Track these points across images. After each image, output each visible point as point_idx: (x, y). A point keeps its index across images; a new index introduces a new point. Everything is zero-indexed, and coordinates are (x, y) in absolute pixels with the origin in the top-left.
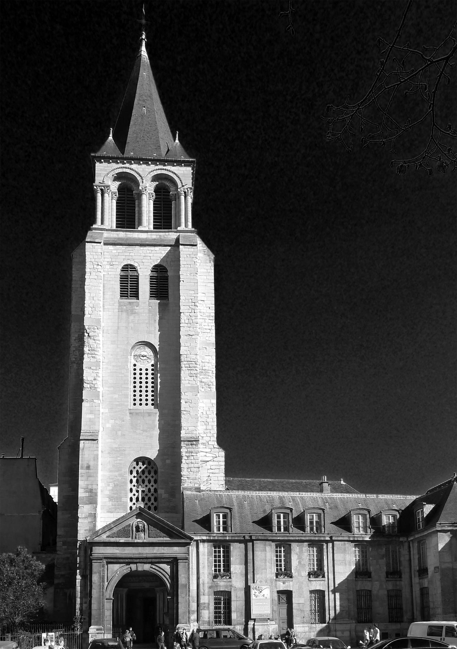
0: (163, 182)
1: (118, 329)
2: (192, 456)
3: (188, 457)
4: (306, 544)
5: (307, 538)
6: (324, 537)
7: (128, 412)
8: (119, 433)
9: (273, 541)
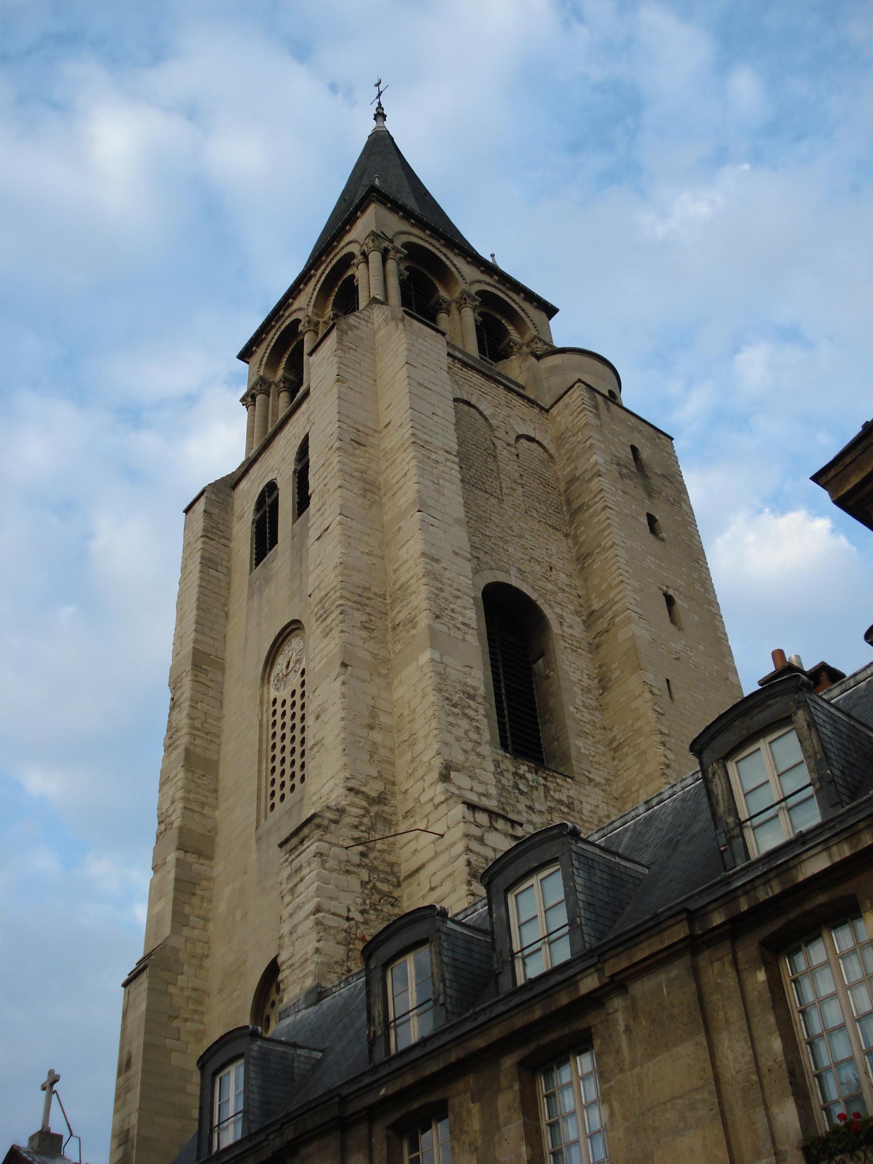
0: (345, 277)
1: (246, 642)
2: (302, 880)
3: (292, 890)
4: (509, 1062)
5: (496, 1033)
6: (571, 982)
7: (254, 840)
8: (238, 915)
9: (372, 1114)
